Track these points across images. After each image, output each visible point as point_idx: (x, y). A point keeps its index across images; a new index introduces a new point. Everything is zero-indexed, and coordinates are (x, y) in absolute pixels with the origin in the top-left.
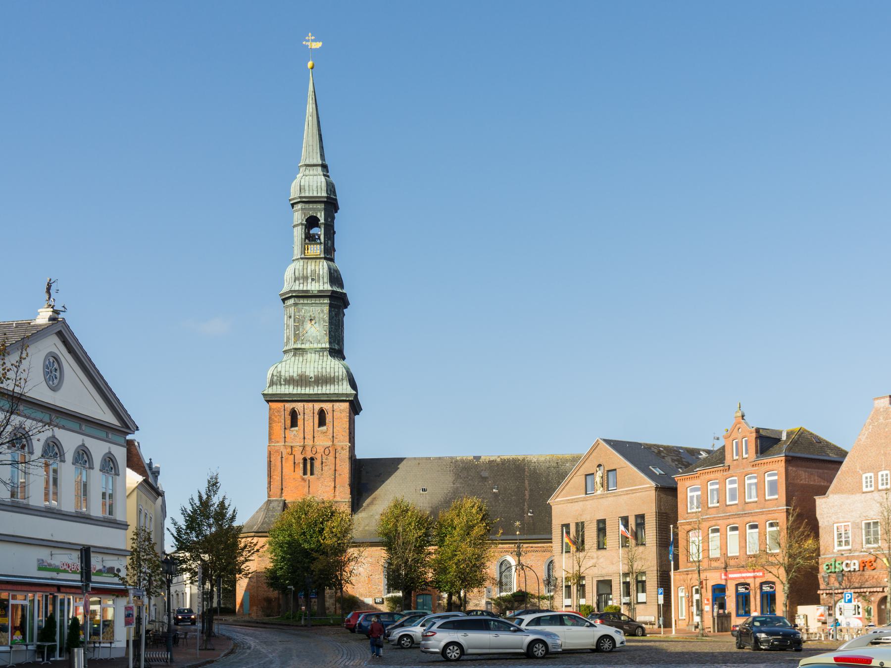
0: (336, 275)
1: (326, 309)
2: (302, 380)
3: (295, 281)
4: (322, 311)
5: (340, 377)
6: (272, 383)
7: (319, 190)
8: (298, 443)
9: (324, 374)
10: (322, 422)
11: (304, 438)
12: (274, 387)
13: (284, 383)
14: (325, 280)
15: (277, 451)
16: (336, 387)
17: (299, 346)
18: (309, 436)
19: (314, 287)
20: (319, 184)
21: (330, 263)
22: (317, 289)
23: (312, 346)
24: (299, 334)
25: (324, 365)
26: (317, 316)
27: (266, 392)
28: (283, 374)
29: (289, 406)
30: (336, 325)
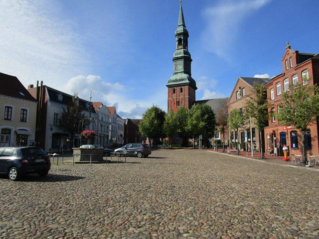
2: (176, 80)
6: (169, 82)
10: (181, 91)
18: (178, 95)
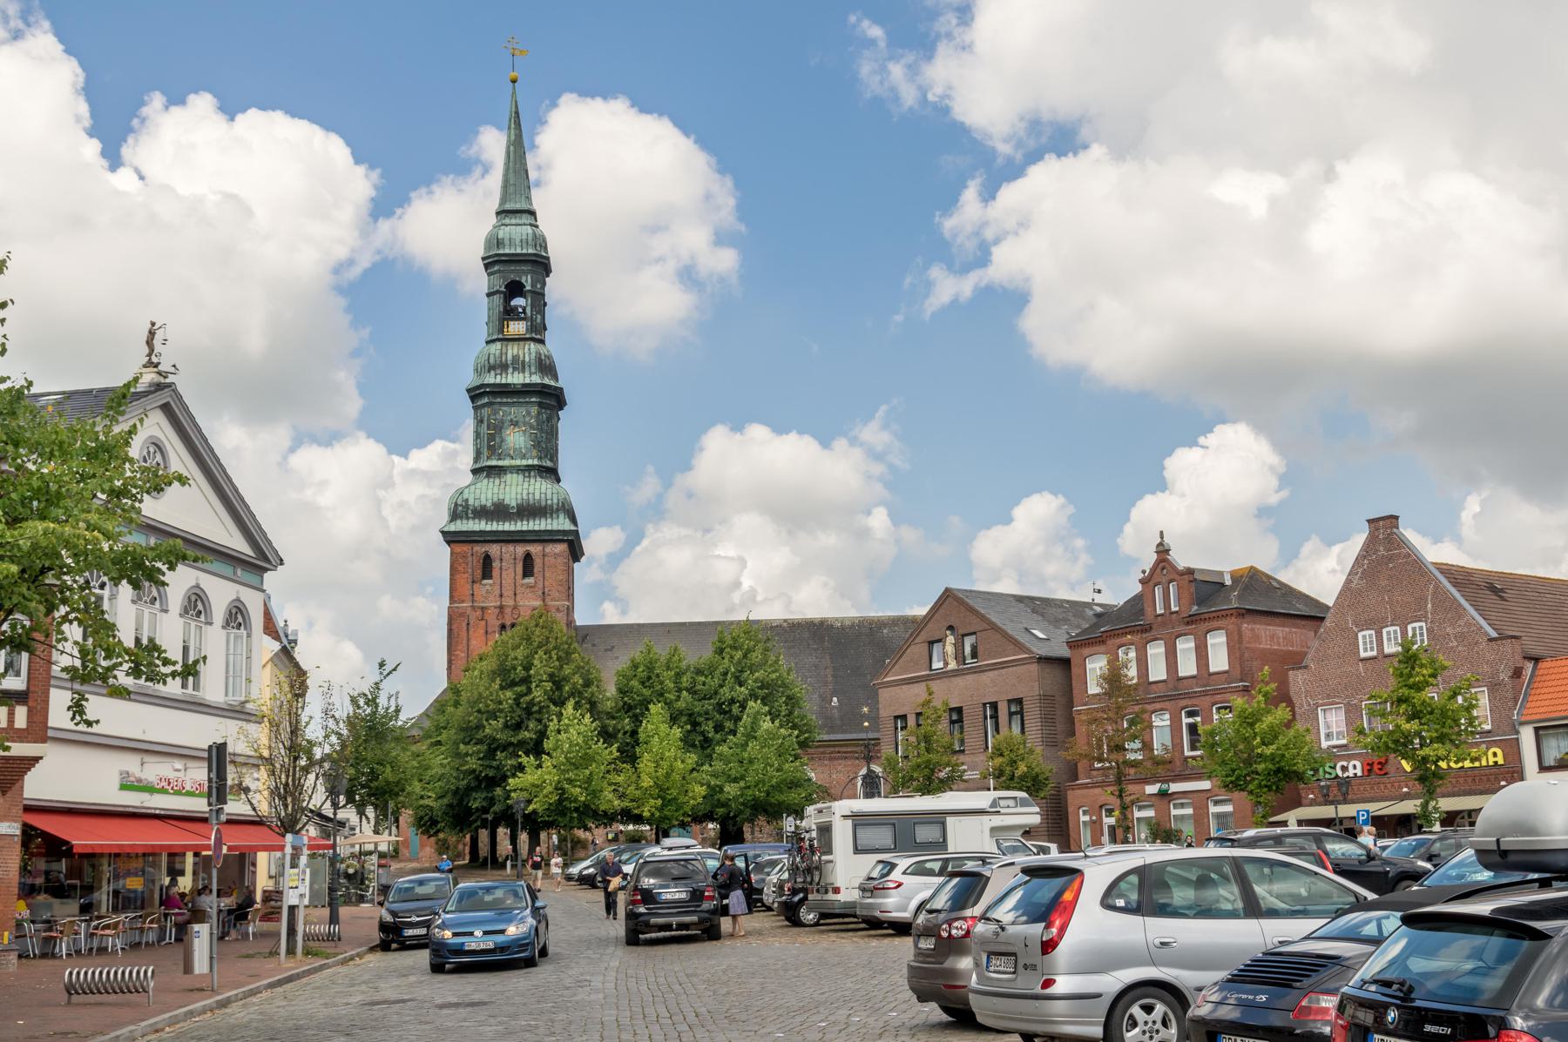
0: (548, 362)
1: (534, 410)
2: (499, 511)
3: (489, 372)
4: (529, 413)
5: (555, 507)
7: (524, 245)
8: (493, 603)
9: (531, 502)
11: (501, 596)
12: (459, 522)
13: (470, 515)
14: (533, 370)
15: (462, 615)
16: (549, 521)
17: (494, 463)
18: (508, 592)
19: (515, 379)
20: (524, 237)
21: (539, 346)
22: (521, 381)
23: (513, 463)
24: (494, 445)
25: (531, 491)
26: (522, 419)
27: (446, 529)
28: (471, 502)
29: (480, 549)
30: (547, 433)
